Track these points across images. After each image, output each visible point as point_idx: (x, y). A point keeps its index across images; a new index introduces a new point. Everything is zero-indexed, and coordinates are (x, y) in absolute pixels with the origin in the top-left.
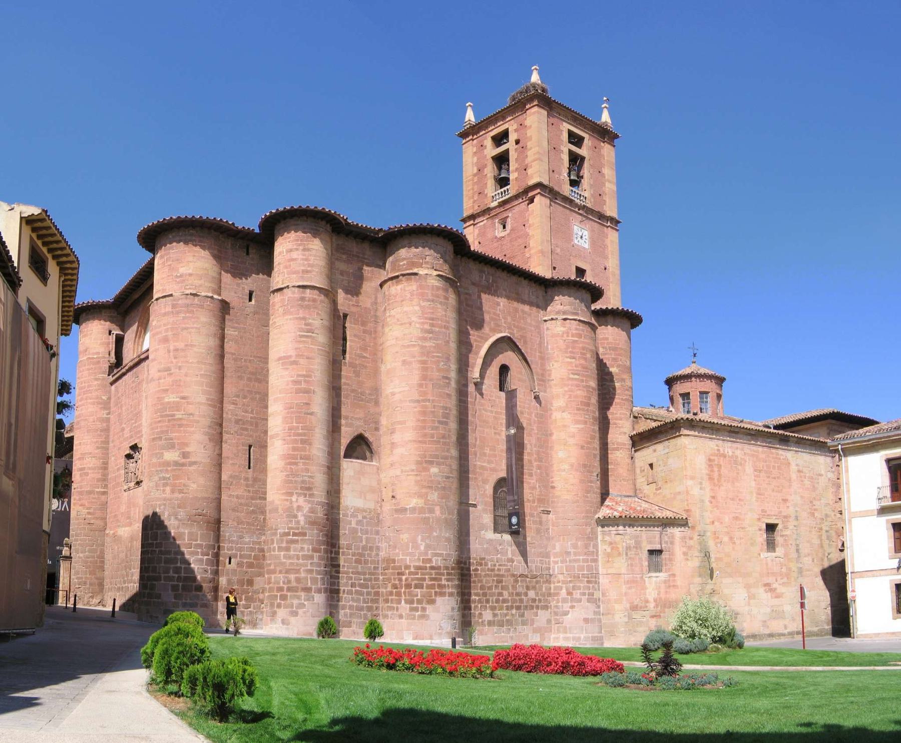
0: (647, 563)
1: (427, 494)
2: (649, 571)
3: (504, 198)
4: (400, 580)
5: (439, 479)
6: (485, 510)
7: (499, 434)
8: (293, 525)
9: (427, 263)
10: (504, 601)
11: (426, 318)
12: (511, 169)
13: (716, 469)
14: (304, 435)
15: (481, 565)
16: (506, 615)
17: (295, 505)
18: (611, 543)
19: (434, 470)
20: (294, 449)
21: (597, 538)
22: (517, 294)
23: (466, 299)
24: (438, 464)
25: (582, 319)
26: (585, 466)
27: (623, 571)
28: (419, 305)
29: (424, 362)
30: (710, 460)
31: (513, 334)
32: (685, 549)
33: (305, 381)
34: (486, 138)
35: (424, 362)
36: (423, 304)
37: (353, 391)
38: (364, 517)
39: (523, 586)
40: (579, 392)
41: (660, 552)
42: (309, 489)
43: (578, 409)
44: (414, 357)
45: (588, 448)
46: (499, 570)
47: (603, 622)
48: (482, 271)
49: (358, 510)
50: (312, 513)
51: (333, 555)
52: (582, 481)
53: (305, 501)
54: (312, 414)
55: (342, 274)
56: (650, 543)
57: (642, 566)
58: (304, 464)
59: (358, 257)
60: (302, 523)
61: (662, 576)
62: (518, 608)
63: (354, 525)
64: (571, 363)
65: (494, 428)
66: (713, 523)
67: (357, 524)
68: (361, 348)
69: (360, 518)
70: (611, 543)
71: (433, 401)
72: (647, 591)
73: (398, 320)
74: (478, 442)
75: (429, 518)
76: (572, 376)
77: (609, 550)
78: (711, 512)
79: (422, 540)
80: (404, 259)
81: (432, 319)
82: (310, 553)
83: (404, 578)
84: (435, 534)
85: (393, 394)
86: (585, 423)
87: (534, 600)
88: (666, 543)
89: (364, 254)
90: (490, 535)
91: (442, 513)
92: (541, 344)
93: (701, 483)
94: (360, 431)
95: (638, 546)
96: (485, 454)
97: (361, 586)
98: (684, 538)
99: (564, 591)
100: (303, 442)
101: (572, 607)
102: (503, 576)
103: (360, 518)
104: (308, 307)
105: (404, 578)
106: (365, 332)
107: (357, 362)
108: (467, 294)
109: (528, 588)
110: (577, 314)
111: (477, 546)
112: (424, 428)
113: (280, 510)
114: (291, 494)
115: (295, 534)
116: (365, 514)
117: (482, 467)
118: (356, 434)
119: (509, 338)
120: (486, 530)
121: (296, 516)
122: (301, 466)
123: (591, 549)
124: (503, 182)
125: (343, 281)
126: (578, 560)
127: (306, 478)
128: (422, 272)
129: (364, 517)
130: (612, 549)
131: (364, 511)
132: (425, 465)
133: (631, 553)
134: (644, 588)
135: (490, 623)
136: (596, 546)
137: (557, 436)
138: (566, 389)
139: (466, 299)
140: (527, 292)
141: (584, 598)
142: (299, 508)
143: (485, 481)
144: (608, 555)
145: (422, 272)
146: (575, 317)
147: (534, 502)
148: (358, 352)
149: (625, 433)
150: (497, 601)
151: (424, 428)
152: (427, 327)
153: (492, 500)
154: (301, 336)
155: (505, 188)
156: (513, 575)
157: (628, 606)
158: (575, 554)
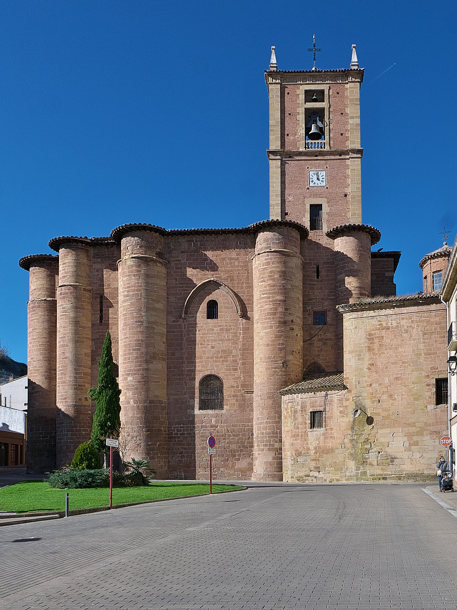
0: (309, 422)
13: (376, 341)
30: (370, 335)
32: (341, 409)
43: (266, 319)
52: (267, 369)
64: (262, 285)
66: (371, 385)
76: (262, 296)
78: (369, 377)
92: (248, 277)
93: (359, 355)
98: (341, 400)
104: (64, 298)
137: (256, 339)
138: (259, 306)
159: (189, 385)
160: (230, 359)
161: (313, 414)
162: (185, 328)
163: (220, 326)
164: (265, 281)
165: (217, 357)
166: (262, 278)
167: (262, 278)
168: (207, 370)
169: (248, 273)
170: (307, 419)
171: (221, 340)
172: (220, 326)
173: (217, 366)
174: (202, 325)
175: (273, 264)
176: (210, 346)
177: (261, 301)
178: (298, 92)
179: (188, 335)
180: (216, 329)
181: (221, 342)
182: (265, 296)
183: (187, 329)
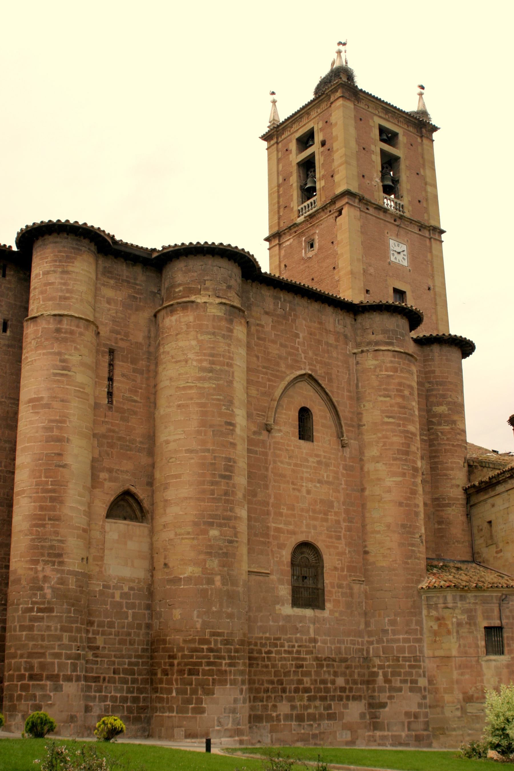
0: (483, 643)
1: (205, 561)
2: (488, 653)
3: (311, 212)
4: (172, 665)
5: (221, 543)
6: (281, 582)
7: (299, 490)
8: (38, 599)
9: (207, 289)
10: (306, 690)
11: (205, 354)
12: (317, 176)
14: (54, 491)
15: (276, 645)
16: (306, 707)
17: (41, 575)
18: (438, 619)
19: (214, 532)
20: (41, 508)
21: (421, 613)
22: (320, 323)
23: (257, 331)
24: (220, 525)
25: (397, 349)
26: (403, 526)
27: (454, 653)
28: (196, 338)
29: (202, 405)
31: (316, 371)
33: (58, 427)
34: (291, 141)
35: (202, 405)
36: (200, 337)
37: (120, 439)
38: (131, 589)
39: (329, 673)
40: (395, 439)
41: (500, 629)
42: (60, 555)
43: (395, 459)
44: (192, 399)
45: (408, 505)
46: (299, 652)
47: (430, 716)
48: (276, 298)
49: (122, 580)
50: (62, 584)
51: (90, 635)
52: (401, 545)
53: (53, 570)
54: (64, 466)
55: (109, 303)
56: (488, 618)
57: (477, 646)
58: (53, 526)
59: (128, 282)
60: (49, 596)
61: (503, 659)
62: (323, 699)
63: (117, 598)
64: (385, 401)
65: (293, 483)
67: (121, 597)
68: (130, 391)
69: (126, 589)
70: (438, 619)
71: (213, 450)
72: (485, 678)
73: (173, 357)
74: (272, 500)
75: (206, 590)
76: (386, 420)
77: (435, 627)
79: (198, 617)
80: (180, 285)
81: (212, 355)
82: (58, 632)
83: (176, 662)
84: (214, 609)
85: (167, 442)
86: (404, 475)
87: (343, 689)
88: (508, 617)
89: (136, 279)
90: (288, 610)
91: (223, 584)
94: (127, 486)
95: (472, 621)
96: (281, 514)
97: (125, 671)
99: (381, 677)
100: (53, 499)
101: (391, 698)
102: (304, 659)
103: (126, 589)
105: (176, 662)
106: (135, 371)
107: (125, 407)
108: (258, 325)
109: (336, 674)
110: (391, 344)
111: (271, 623)
112: (203, 483)
113: (24, 582)
114: (37, 562)
115: (40, 610)
116: (132, 585)
117: (278, 530)
118: (121, 490)
119: (310, 376)
120: (283, 605)
121: (41, 589)
122: (49, 528)
123: (413, 626)
124: (308, 192)
125: (109, 310)
126: (398, 640)
127: (55, 543)
128: (200, 300)
129: (131, 589)
130: (440, 626)
131: (132, 580)
132: (202, 527)
133: (464, 630)
134: (480, 674)
135: (288, 717)
136: (419, 623)
138: (380, 435)
139: (257, 331)
140: (331, 320)
141: (406, 686)
142: (46, 579)
143: (281, 546)
144: (436, 634)
145: (200, 300)
146: (390, 348)
147: (342, 570)
148: (127, 395)
149: (458, 486)
150: (297, 690)
151: (203, 483)
152: (205, 364)
153: (289, 569)
154: (55, 375)
155: (312, 200)
156: (317, 659)
157: (461, 696)
158: (394, 632)
159: (277, 557)
160: (331, 517)
161: (488, 629)
162: (270, 449)
163: (317, 456)
164: (389, 396)
165: (314, 511)
166: (385, 389)
167: (385, 389)
168: (302, 532)
169: (349, 374)
170: (479, 637)
171: (319, 482)
172: (317, 456)
173: (315, 527)
174: (292, 448)
175: (402, 371)
176: (304, 490)
177: (385, 427)
178: (371, 123)
179: (275, 462)
180: (311, 459)
181: (318, 485)
182: (391, 420)
183: (272, 450)
